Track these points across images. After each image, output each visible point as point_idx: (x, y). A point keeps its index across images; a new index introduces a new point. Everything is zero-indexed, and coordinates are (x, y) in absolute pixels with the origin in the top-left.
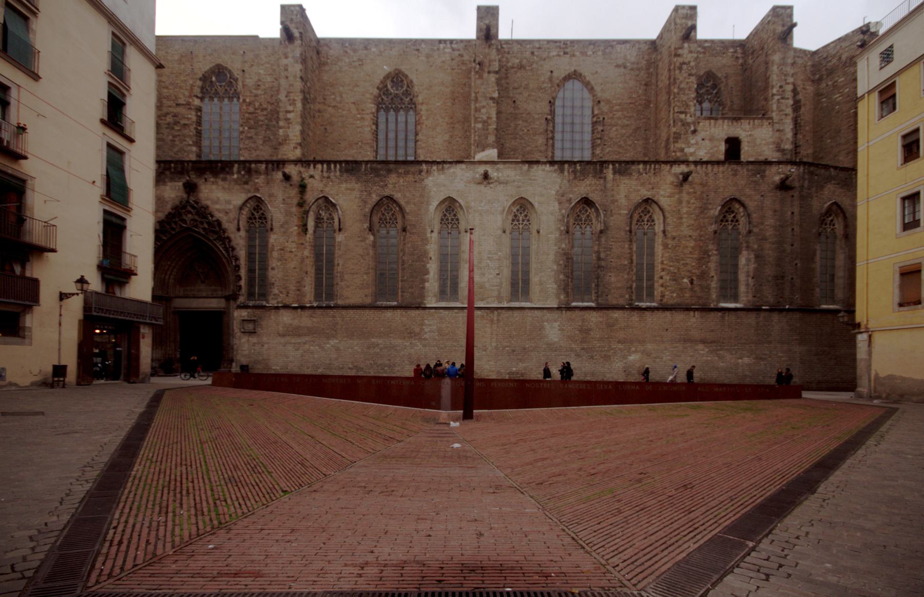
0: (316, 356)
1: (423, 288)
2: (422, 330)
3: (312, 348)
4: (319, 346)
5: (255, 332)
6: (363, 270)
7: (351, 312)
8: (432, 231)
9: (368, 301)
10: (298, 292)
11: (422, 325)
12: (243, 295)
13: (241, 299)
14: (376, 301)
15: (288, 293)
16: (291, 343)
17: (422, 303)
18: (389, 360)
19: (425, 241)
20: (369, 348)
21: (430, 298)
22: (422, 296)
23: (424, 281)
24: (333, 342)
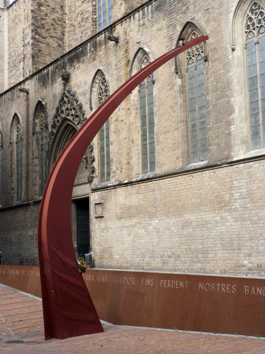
0: (143, 241)
1: (229, 134)
2: (232, 195)
3: (139, 231)
4: (144, 228)
5: (102, 217)
6: (173, 125)
7: (167, 181)
8: (233, 50)
9: (179, 165)
10: (128, 166)
11: (231, 188)
12: (97, 177)
13: (96, 181)
14: (189, 163)
15: (122, 168)
16: (125, 227)
17: (229, 156)
18: (202, 244)
19: (227, 66)
20: (183, 228)
21: (237, 147)
22: (229, 147)
23: (229, 124)
24: (155, 222)
